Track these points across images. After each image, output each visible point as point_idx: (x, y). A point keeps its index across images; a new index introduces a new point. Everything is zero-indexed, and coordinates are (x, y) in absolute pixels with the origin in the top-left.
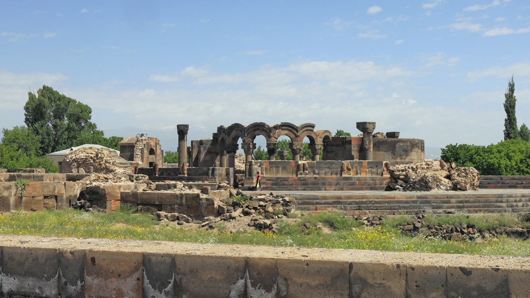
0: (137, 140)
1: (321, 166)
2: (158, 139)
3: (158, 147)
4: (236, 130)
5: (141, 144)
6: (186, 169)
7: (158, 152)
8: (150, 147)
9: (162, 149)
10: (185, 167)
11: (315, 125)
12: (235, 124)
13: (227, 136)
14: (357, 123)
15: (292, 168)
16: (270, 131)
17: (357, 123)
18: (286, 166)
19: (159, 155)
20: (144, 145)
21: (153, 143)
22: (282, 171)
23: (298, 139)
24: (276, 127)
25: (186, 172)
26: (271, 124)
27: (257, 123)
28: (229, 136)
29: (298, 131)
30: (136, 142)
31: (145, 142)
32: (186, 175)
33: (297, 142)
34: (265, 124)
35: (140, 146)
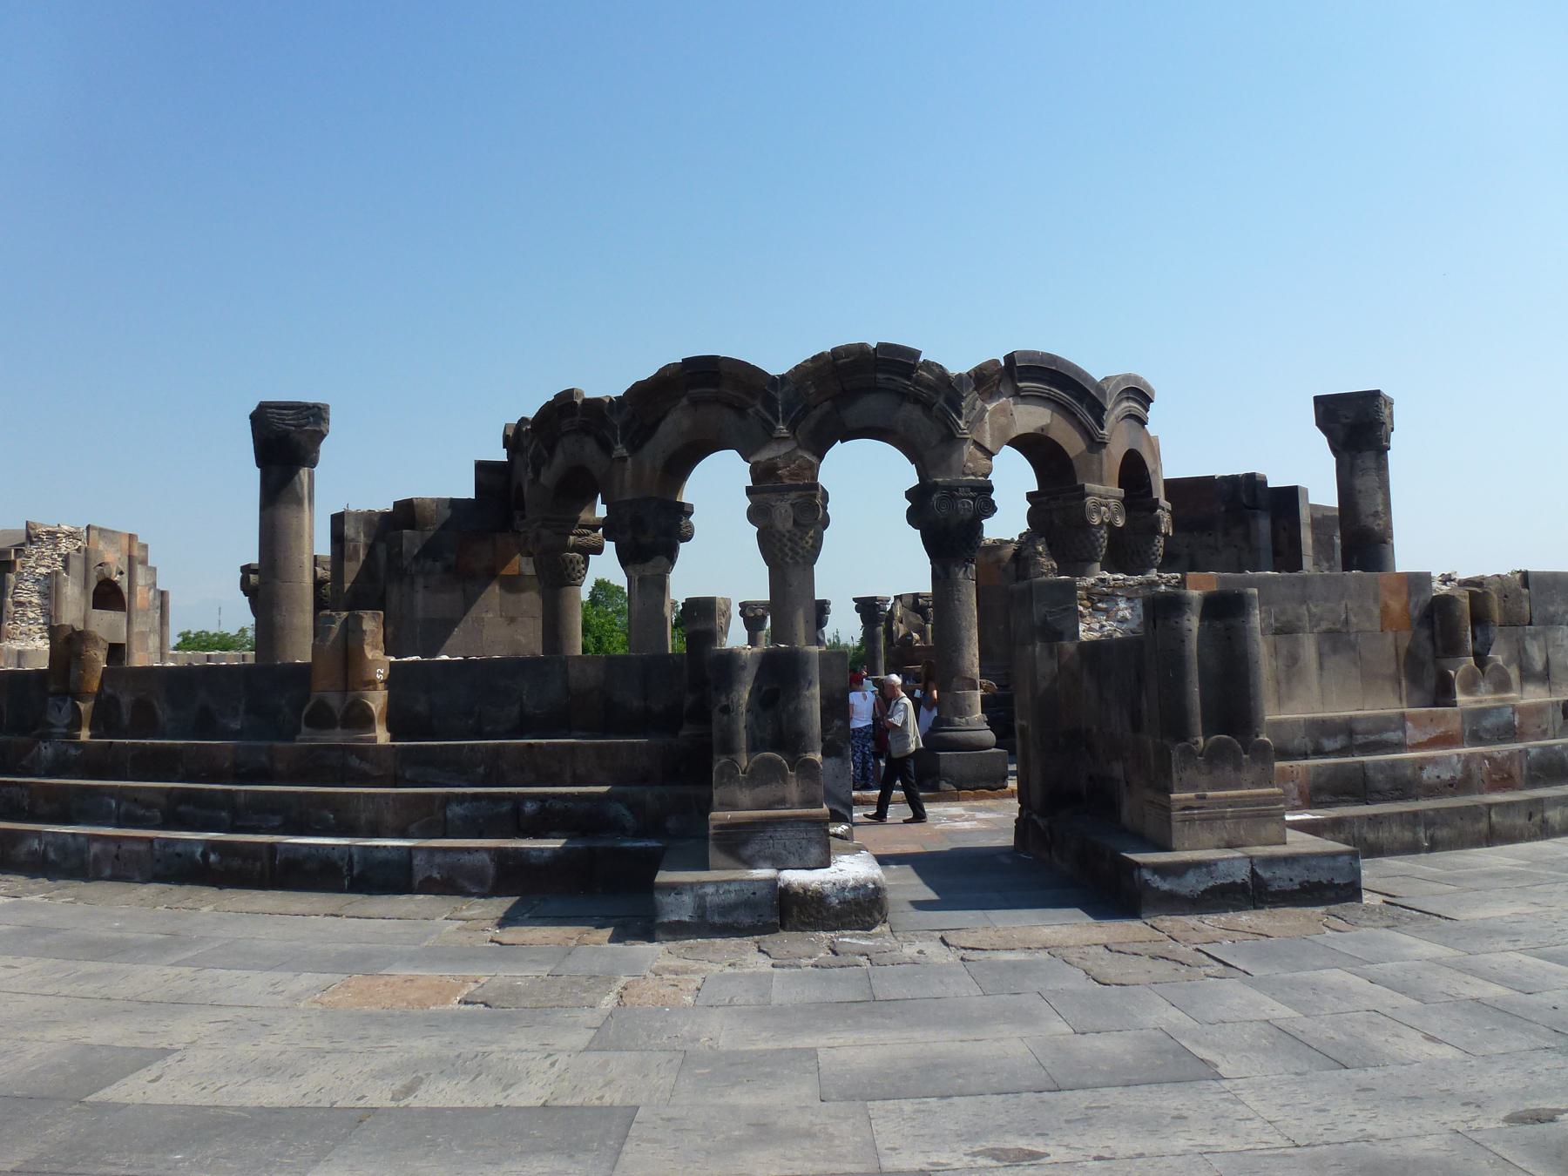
0: (29, 536)
1: (1552, 609)
2: (141, 540)
3: (141, 579)
4: (695, 403)
5: (48, 553)
6: (381, 674)
7: (143, 597)
8: (101, 572)
9: (160, 587)
10: (370, 654)
11: (1153, 392)
12: (689, 363)
13: (620, 450)
14: (1320, 401)
15: (1390, 637)
16: (955, 403)
17: (1320, 401)
18: (1347, 621)
19: (146, 612)
20: (66, 559)
21: (113, 558)
22: (1321, 666)
23: (1101, 463)
24: (989, 379)
25: (377, 701)
26: (958, 363)
27: (862, 346)
28: (635, 447)
29: (1103, 409)
30: (23, 544)
31: (65, 546)
32: (382, 736)
33: (1101, 482)
34: (915, 354)
35: (40, 563)
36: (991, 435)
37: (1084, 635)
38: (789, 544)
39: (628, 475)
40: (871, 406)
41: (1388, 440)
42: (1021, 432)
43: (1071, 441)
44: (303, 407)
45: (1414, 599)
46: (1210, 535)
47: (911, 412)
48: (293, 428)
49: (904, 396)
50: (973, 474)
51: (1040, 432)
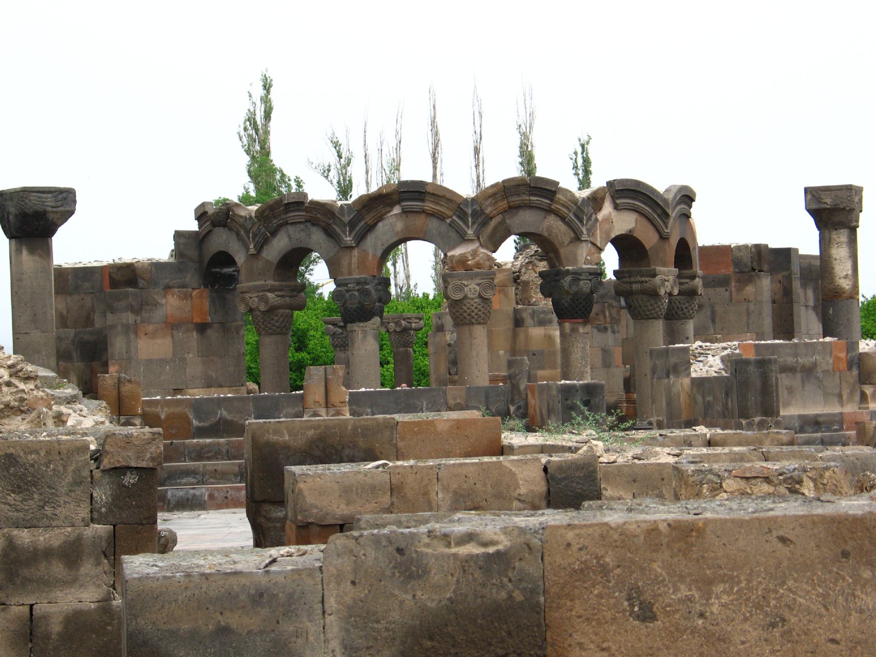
11: (694, 194)
14: (807, 190)
28: (361, 238)
36: (601, 237)
37: (694, 375)
38: (476, 311)
39: (354, 260)
40: (527, 219)
41: (857, 221)
42: (618, 233)
43: (648, 237)
44: (55, 192)
45: (850, 354)
46: (727, 290)
47: (552, 221)
48: (50, 209)
49: (549, 211)
50: (590, 264)
51: (629, 233)
